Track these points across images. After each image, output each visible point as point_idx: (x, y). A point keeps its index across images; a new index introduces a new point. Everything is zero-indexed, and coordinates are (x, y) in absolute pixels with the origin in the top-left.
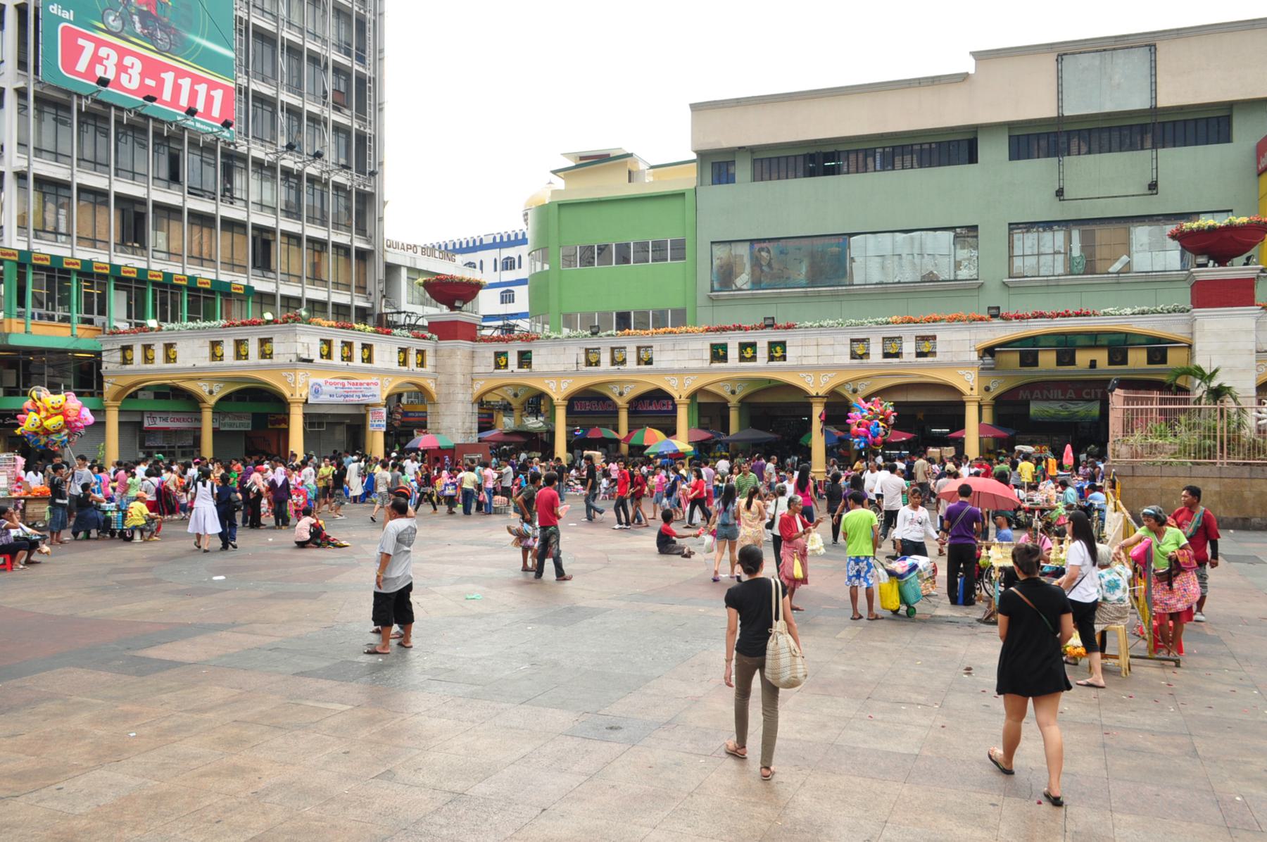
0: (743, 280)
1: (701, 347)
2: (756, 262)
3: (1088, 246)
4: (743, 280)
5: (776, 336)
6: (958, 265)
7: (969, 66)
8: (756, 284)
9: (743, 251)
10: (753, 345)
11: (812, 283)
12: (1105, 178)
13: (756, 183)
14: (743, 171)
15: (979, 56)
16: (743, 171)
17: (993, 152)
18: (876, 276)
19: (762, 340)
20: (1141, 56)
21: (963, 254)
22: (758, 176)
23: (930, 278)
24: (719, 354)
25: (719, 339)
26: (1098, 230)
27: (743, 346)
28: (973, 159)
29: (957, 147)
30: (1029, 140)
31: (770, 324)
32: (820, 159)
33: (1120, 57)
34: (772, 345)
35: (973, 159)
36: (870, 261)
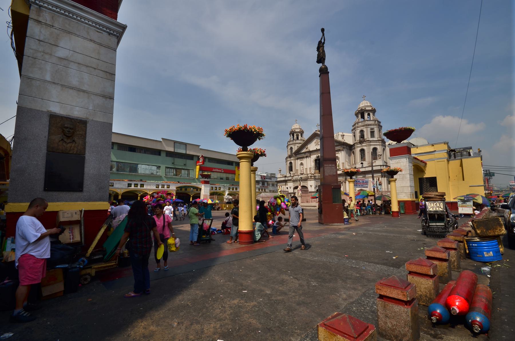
0: (114, 169)
1: (126, 183)
2: (118, 166)
3: (176, 172)
4: (114, 169)
5: (142, 183)
6: (157, 172)
7: (162, 140)
8: (118, 170)
9: (115, 164)
10: (137, 184)
11: (130, 172)
12: (180, 163)
13: (120, 151)
14: (115, 147)
15: (163, 139)
16: (115, 147)
17: (163, 154)
18: (143, 172)
19: (139, 183)
20: (184, 146)
21: (158, 170)
22: (119, 149)
23: (152, 174)
24: (130, 185)
25: (130, 182)
26: (178, 171)
27: (135, 184)
28: (160, 155)
29: (158, 152)
30: (169, 154)
31: (141, 180)
32: (132, 149)
33: (182, 145)
34: (141, 184)
35: (160, 155)
36: (143, 169)
